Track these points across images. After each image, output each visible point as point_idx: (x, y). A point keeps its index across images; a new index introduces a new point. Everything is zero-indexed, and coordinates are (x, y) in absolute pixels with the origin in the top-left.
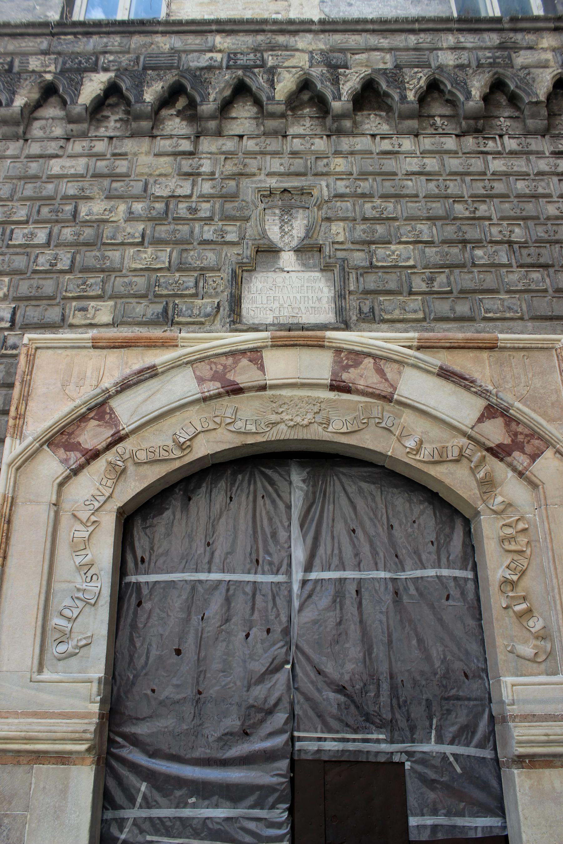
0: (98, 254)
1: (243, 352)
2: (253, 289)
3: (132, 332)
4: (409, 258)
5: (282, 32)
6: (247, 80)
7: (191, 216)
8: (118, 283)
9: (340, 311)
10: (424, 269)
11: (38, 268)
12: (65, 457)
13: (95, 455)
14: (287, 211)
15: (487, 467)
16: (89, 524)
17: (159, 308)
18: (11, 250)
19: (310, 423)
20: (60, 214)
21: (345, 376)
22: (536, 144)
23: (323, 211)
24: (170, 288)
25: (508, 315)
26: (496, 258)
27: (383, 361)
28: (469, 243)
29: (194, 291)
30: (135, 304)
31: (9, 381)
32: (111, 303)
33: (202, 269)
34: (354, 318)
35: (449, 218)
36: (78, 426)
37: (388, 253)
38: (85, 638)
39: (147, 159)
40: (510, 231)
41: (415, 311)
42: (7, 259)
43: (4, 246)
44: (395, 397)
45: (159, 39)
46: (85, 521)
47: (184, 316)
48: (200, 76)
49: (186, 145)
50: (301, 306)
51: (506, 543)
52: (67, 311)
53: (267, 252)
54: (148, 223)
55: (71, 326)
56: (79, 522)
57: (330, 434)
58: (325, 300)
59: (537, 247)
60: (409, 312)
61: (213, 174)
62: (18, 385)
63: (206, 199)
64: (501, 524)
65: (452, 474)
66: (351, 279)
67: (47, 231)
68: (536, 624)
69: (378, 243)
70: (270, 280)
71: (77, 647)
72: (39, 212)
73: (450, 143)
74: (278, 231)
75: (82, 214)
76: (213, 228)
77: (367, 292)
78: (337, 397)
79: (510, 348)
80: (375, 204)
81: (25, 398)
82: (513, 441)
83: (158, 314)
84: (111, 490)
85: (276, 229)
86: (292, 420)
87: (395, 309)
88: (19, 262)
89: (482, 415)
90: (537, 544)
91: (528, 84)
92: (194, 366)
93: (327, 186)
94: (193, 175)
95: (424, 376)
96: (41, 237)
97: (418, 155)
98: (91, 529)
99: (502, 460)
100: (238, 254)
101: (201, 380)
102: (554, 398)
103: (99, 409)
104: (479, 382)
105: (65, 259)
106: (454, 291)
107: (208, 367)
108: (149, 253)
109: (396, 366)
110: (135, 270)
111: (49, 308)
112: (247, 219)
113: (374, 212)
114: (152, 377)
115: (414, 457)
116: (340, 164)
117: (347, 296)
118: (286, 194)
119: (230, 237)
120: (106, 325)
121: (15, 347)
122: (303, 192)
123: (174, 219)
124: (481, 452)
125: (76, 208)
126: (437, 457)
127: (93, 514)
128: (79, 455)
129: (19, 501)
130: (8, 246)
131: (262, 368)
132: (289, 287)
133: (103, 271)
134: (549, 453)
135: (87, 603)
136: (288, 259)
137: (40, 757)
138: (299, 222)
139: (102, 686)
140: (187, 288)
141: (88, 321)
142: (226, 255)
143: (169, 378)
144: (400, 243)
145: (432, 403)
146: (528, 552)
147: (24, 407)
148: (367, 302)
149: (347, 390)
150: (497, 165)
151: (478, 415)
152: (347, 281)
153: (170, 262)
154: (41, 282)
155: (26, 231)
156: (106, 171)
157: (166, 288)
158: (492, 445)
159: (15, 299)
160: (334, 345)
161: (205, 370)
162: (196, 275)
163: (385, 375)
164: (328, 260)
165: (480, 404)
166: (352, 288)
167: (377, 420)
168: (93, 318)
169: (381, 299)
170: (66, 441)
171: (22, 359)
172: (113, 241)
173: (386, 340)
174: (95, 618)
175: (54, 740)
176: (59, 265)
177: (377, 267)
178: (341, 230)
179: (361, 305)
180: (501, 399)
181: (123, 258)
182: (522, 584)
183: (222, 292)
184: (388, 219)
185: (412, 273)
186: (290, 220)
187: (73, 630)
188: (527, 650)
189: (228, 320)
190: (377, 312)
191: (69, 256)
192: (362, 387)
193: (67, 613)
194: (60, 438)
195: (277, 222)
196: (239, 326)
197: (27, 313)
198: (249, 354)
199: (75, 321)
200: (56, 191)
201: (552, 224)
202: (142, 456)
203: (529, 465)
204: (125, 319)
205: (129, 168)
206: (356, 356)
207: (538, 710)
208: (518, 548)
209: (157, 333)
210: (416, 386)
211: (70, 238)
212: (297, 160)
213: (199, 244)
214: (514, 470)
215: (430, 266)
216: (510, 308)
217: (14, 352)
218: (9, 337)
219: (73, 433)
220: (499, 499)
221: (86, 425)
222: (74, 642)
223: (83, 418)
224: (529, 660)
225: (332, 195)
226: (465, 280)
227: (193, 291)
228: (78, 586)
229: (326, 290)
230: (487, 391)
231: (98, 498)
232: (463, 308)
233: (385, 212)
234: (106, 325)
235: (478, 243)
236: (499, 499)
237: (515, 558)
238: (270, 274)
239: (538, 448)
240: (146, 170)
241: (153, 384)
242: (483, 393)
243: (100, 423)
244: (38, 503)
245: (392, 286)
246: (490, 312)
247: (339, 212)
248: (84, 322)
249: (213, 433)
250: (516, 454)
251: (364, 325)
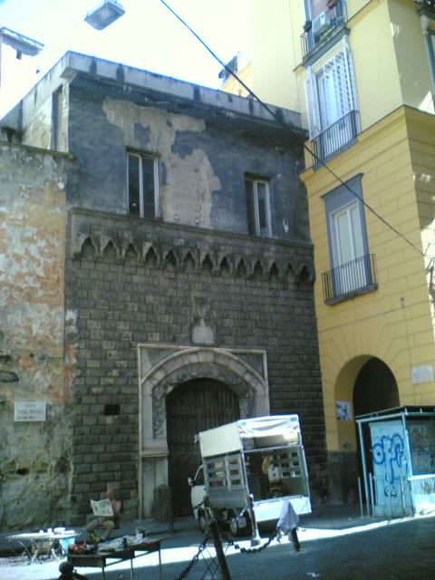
5: (201, 233)
6: (192, 254)
9: (215, 341)
22: (266, 285)
39: (162, 279)
45: (164, 230)
48: (178, 249)
49: (173, 276)
53: (197, 320)
73: (243, 282)
91: (266, 264)
94: (176, 288)
97: (234, 285)
116: (215, 288)
136: (202, 321)
150: (255, 292)
206: (217, 355)
209: (172, 346)
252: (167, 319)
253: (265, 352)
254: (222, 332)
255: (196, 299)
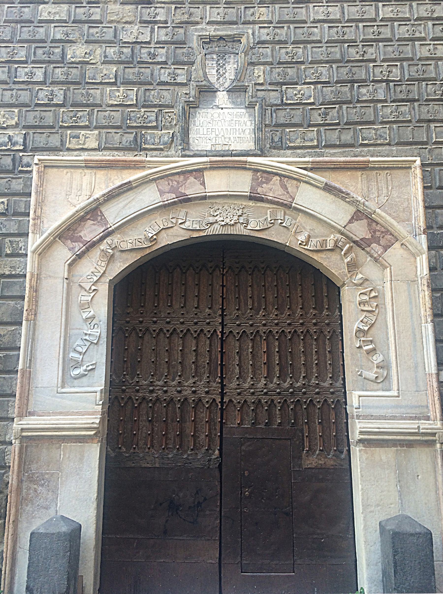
0: (84, 91)
1: (191, 172)
2: (197, 123)
3: (113, 156)
4: (311, 96)
7: (151, 61)
8: (100, 117)
9: (258, 141)
10: (320, 105)
11: (39, 102)
12: (72, 246)
13: (93, 245)
14: (222, 55)
15: (353, 254)
16: (91, 291)
17: (131, 137)
18: (17, 86)
19: (236, 223)
20: (52, 56)
21: (259, 190)
23: (249, 57)
24: (138, 121)
25: (379, 142)
26: (375, 95)
27: (286, 179)
28: (356, 83)
29: (155, 124)
30: (113, 133)
31: (27, 191)
32: (96, 132)
33: (160, 106)
34: (268, 146)
35: (342, 61)
36: (80, 225)
37: (295, 92)
38: (91, 365)
40: (389, 72)
41: (312, 140)
42: (14, 94)
43: (12, 82)
44: (293, 205)
46: (88, 289)
47: (148, 144)
50: (231, 136)
51: (362, 306)
52: (64, 137)
53: (206, 92)
54: (119, 65)
55: (69, 149)
56: (83, 290)
57: (248, 231)
58: (247, 132)
59: (408, 84)
60: (307, 141)
61: (166, 22)
62: (33, 194)
63: (161, 46)
64: (359, 293)
65: (329, 258)
66: (267, 115)
67: (43, 70)
68: (378, 358)
69: (288, 84)
70: (209, 115)
71: (86, 370)
72: (35, 53)
74: (216, 73)
75: (69, 57)
76: (167, 71)
77: (277, 125)
78: (254, 204)
79: (377, 168)
80: (288, 50)
81: (40, 204)
82: (372, 236)
83: (130, 142)
84: (104, 269)
85: (214, 72)
86: (223, 221)
87: (297, 139)
88: (25, 97)
89: (353, 218)
90: (383, 306)
92: (157, 182)
93: (253, 34)
95: (314, 189)
96: (39, 76)
98: (92, 295)
99: (363, 249)
100: (186, 94)
101: (162, 193)
102: (405, 204)
103: (93, 212)
104: (352, 194)
105: (59, 95)
106: (341, 123)
107: (167, 183)
108: (121, 92)
109: (295, 182)
110: (112, 106)
111: (51, 135)
112: (192, 63)
113: (287, 57)
114: (128, 190)
115: (303, 247)
117: (263, 129)
118: (222, 42)
119: (180, 80)
120: (94, 150)
121: (29, 165)
122: (235, 39)
123: (139, 62)
124: (349, 243)
125: (63, 49)
126: (319, 248)
127: (93, 285)
128: (81, 245)
129: (43, 276)
130: (15, 83)
131: (203, 184)
132: (223, 121)
133: (88, 105)
134: (397, 245)
135: (92, 343)
136: (222, 97)
137: (64, 439)
138: (230, 66)
139: (103, 395)
140: (150, 122)
141: (81, 146)
142: (178, 94)
143: (140, 190)
144: (305, 83)
145: (318, 210)
146: (377, 312)
147: (40, 210)
148: (278, 133)
149: (261, 200)
151: (350, 217)
152: (264, 116)
153: (136, 100)
154: (43, 114)
155: (26, 70)
156: (83, 18)
157: (135, 121)
158: (358, 239)
159: (24, 127)
160: (253, 167)
161: (165, 185)
162: (156, 110)
163: (287, 189)
164: (251, 100)
165: (352, 209)
166: (267, 123)
167: (280, 221)
168: (84, 144)
169: (288, 130)
170: (72, 235)
171: (35, 175)
172: (94, 81)
173: (288, 163)
174: (97, 352)
175: (74, 429)
176: (54, 100)
177: (287, 104)
178: (261, 74)
179: (273, 135)
180: (366, 207)
181: (102, 96)
182: (371, 332)
183: (176, 125)
184: (297, 63)
185: (311, 109)
186: (224, 65)
187: (84, 360)
188: (372, 375)
189: (180, 147)
190: (284, 141)
191: (62, 92)
192: (271, 198)
193: (79, 349)
194: (67, 232)
195: (215, 65)
196: (187, 153)
197: (35, 139)
198: (194, 173)
199: (71, 146)
200: (47, 35)
201: (422, 65)
202: (124, 246)
203: (382, 253)
204: (107, 145)
205: (101, 15)
206: (268, 174)
207: (375, 412)
208: (370, 309)
209: (130, 157)
210: (308, 198)
211: (62, 78)
212: (231, 9)
213: (157, 85)
214: (371, 256)
215: (325, 103)
216: (381, 136)
217: (29, 169)
218: (23, 157)
219: (76, 229)
220: (360, 276)
221: (85, 224)
222: (85, 367)
223: (82, 219)
224: (372, 381)
225: (256, 42)
226: (349, 113)
227: (154, 124)
228: (85, 332)
229: (249, 123)
230: (357, 201)
231: (95, 274)
232: (347, 137)
233: (295, 57)
234: (94, 150)
235: (363, 82)
236: (360, 276)
237: (367, 315)
238: (209, 110)
239: (390, 241)
240: (115, 18)
241: (130, 195)
242: (354, 202)
243: (95, 222)
244: (55, 278)
245: (296, 120)
246: (366, 140)
247: (261, 57)
248: (77, 147)
249: (171, 230)
250: (374, 245)
251: (275, 151)
252: (118, 94)
253: (418, 162)
254: (282, 117)
255: (208, 41)
